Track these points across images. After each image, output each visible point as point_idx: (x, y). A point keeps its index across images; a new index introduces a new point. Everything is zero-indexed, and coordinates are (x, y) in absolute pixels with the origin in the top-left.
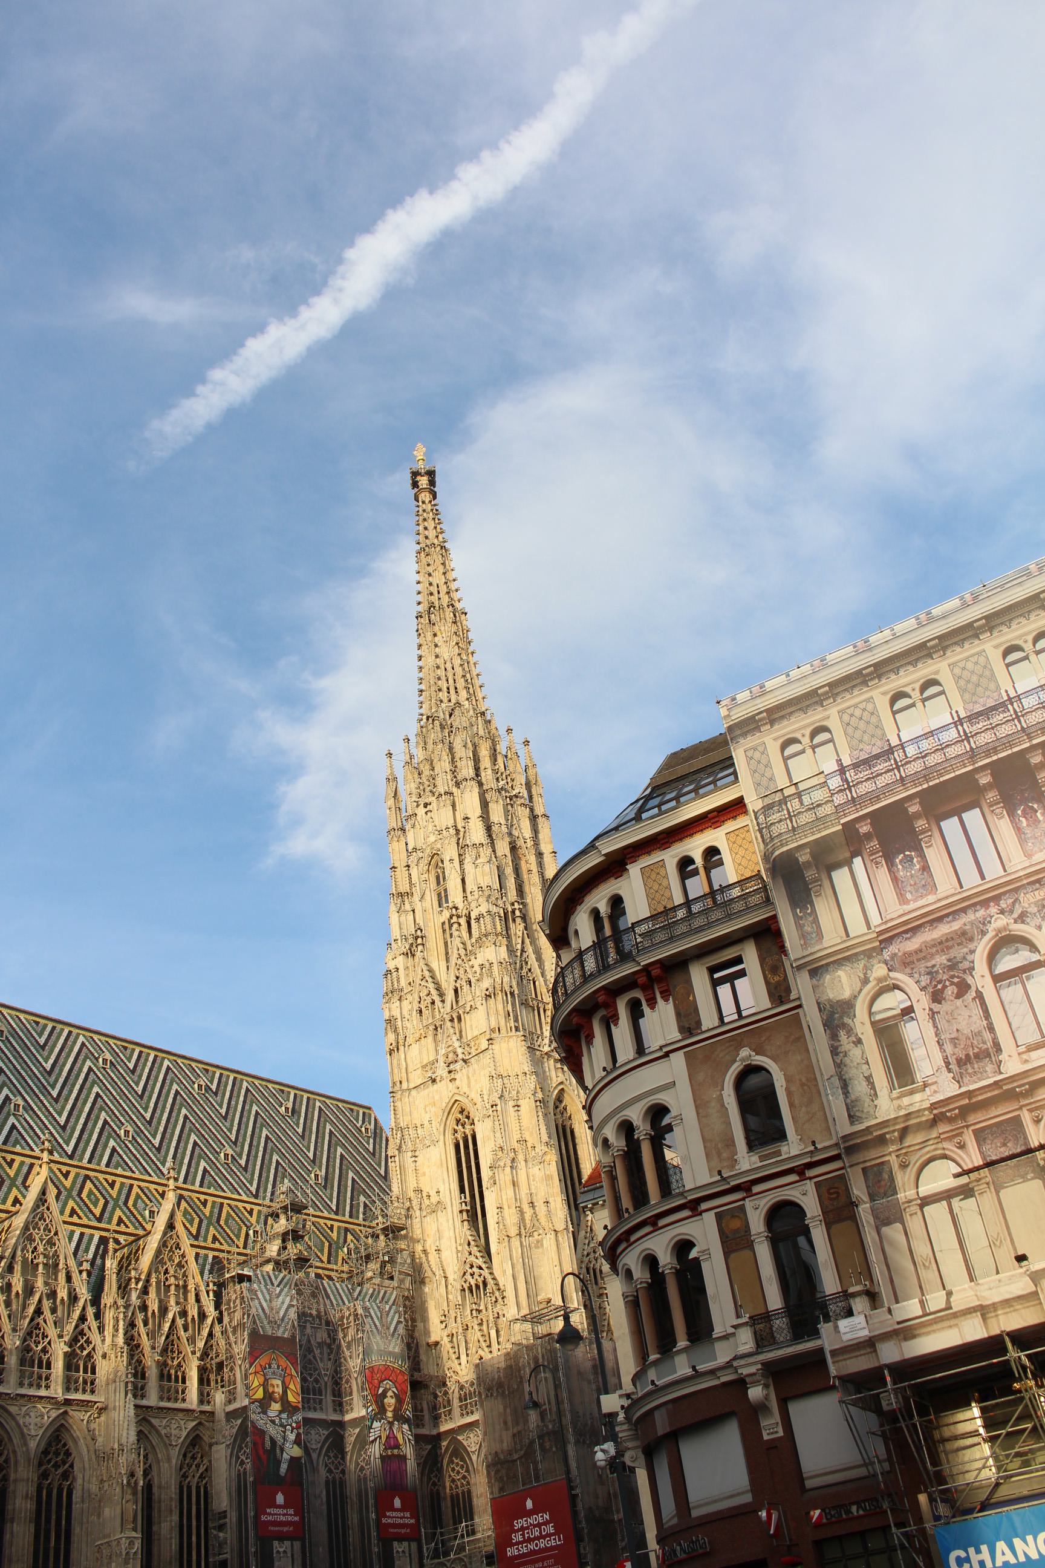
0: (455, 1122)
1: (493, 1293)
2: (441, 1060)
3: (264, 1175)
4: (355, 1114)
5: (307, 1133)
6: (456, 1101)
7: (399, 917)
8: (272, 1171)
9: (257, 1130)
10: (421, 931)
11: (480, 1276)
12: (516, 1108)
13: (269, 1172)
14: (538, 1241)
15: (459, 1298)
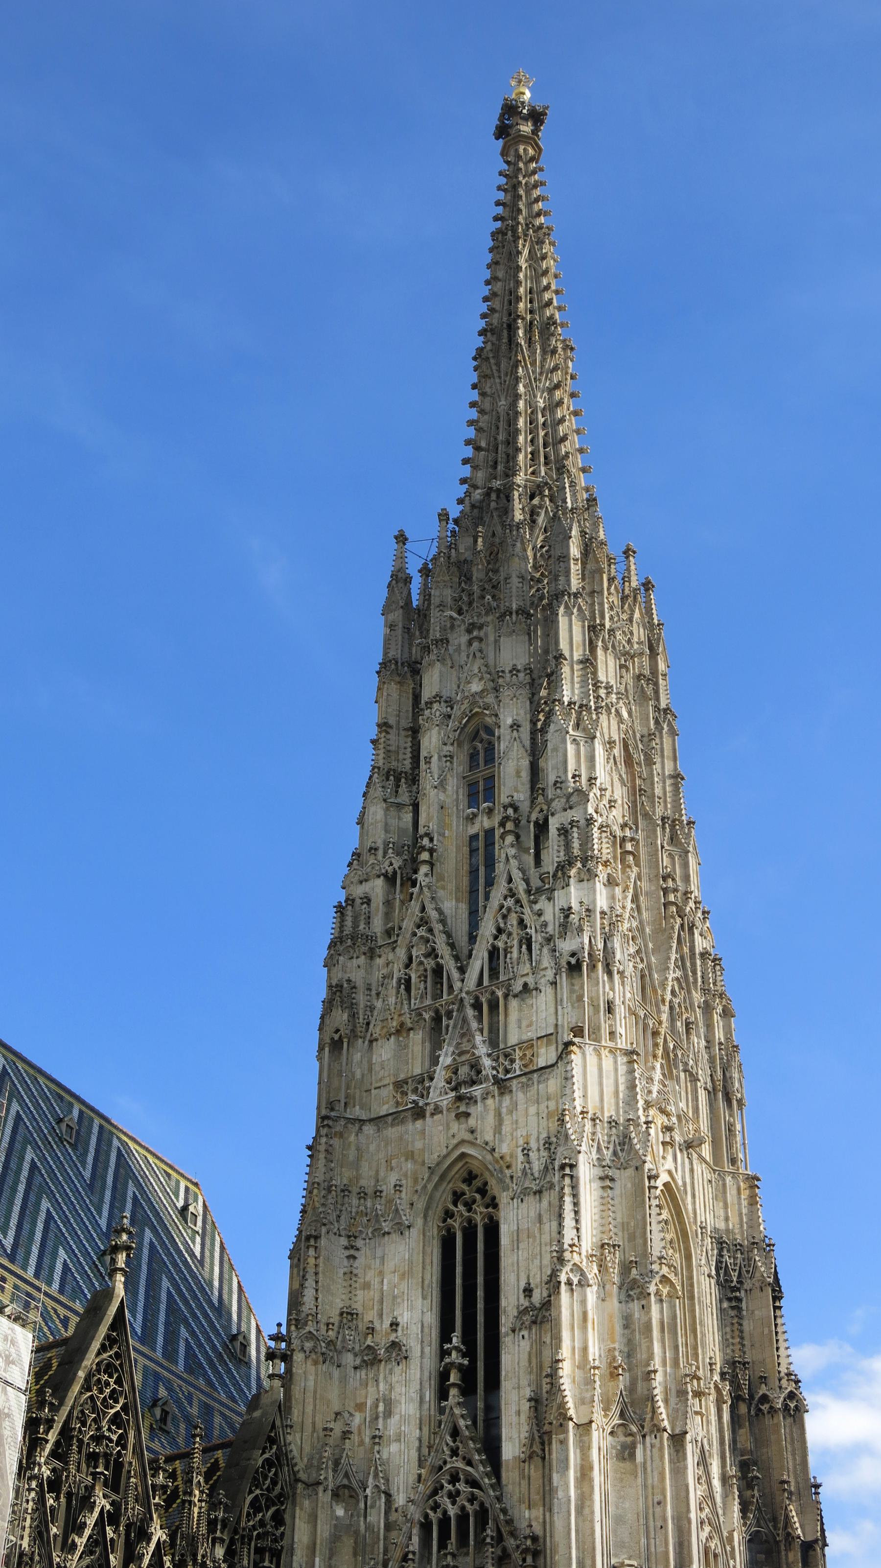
0: (450, 1198)
1: (500, 1538)
2: (441, 1075)
3: (26, 1226)
4: (173, 1183)
5: (98, 1184)
6: (463, 1155)
7: (387, 809)
8: (40, 1226)
9: (18, 1146)
10: (431, 840)
11: (472, 1499)
12: (608, 1183)
13: (34, 1224)
14: (624, 1446)
15: (415, 1539)
